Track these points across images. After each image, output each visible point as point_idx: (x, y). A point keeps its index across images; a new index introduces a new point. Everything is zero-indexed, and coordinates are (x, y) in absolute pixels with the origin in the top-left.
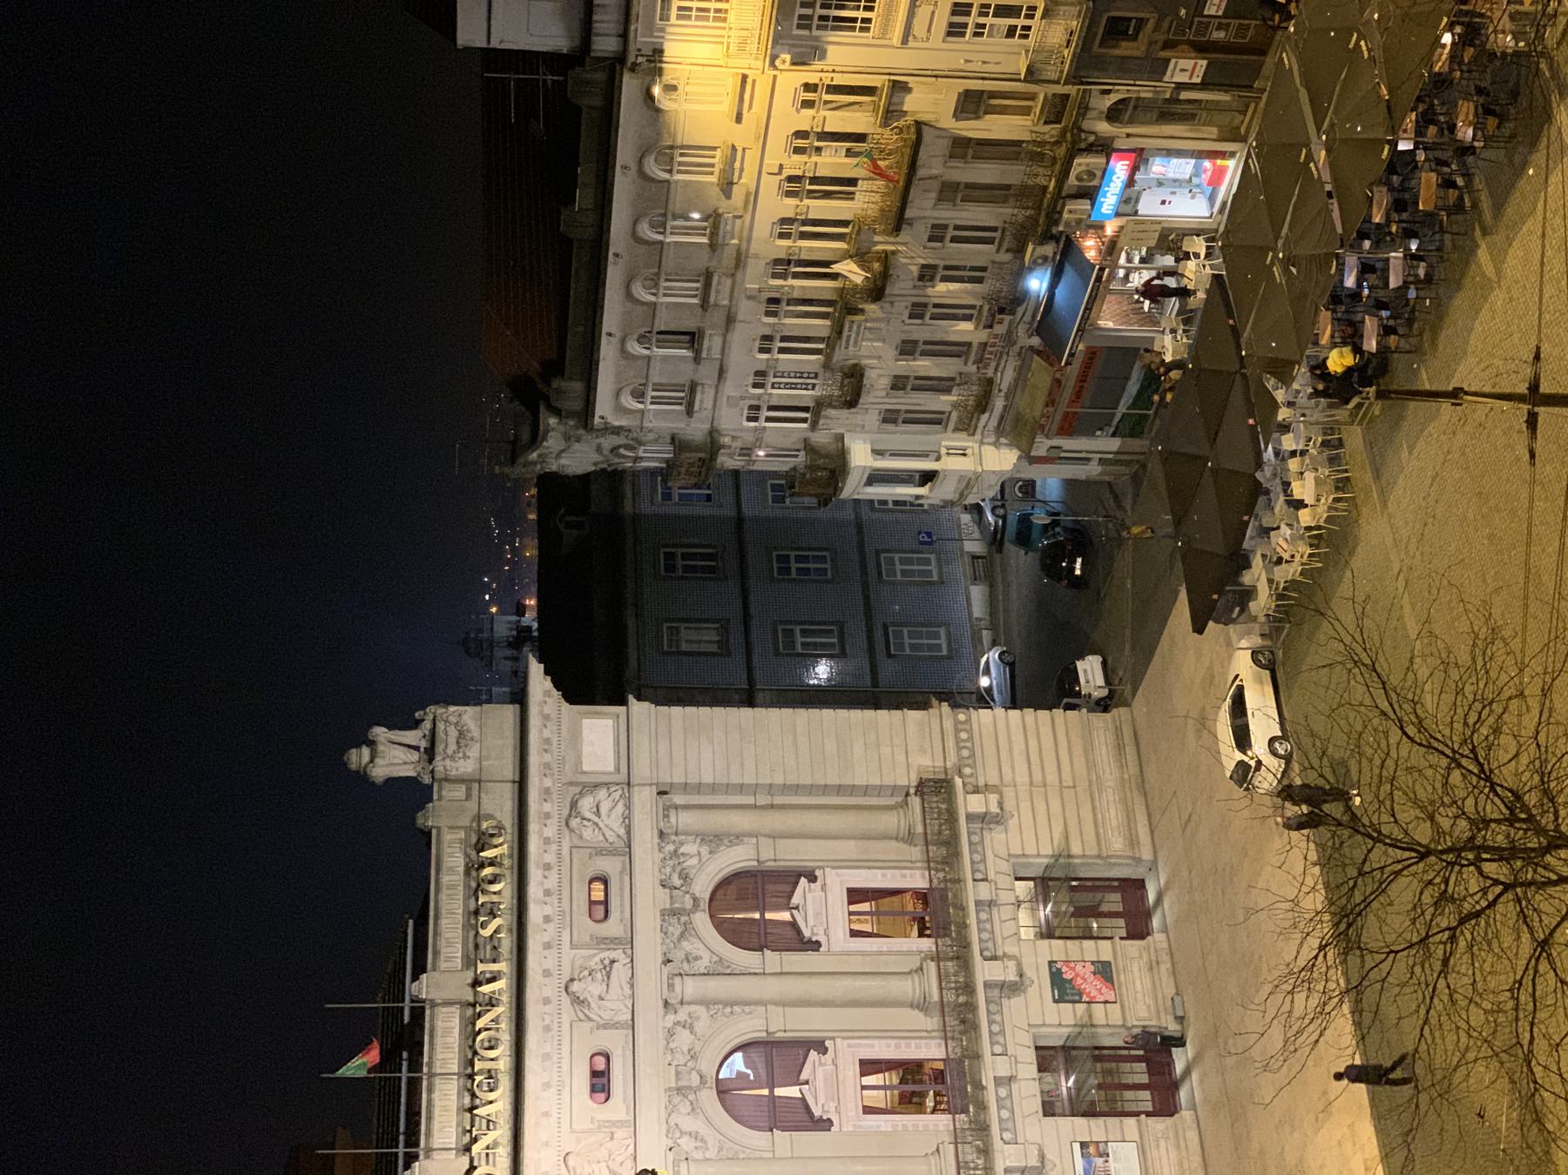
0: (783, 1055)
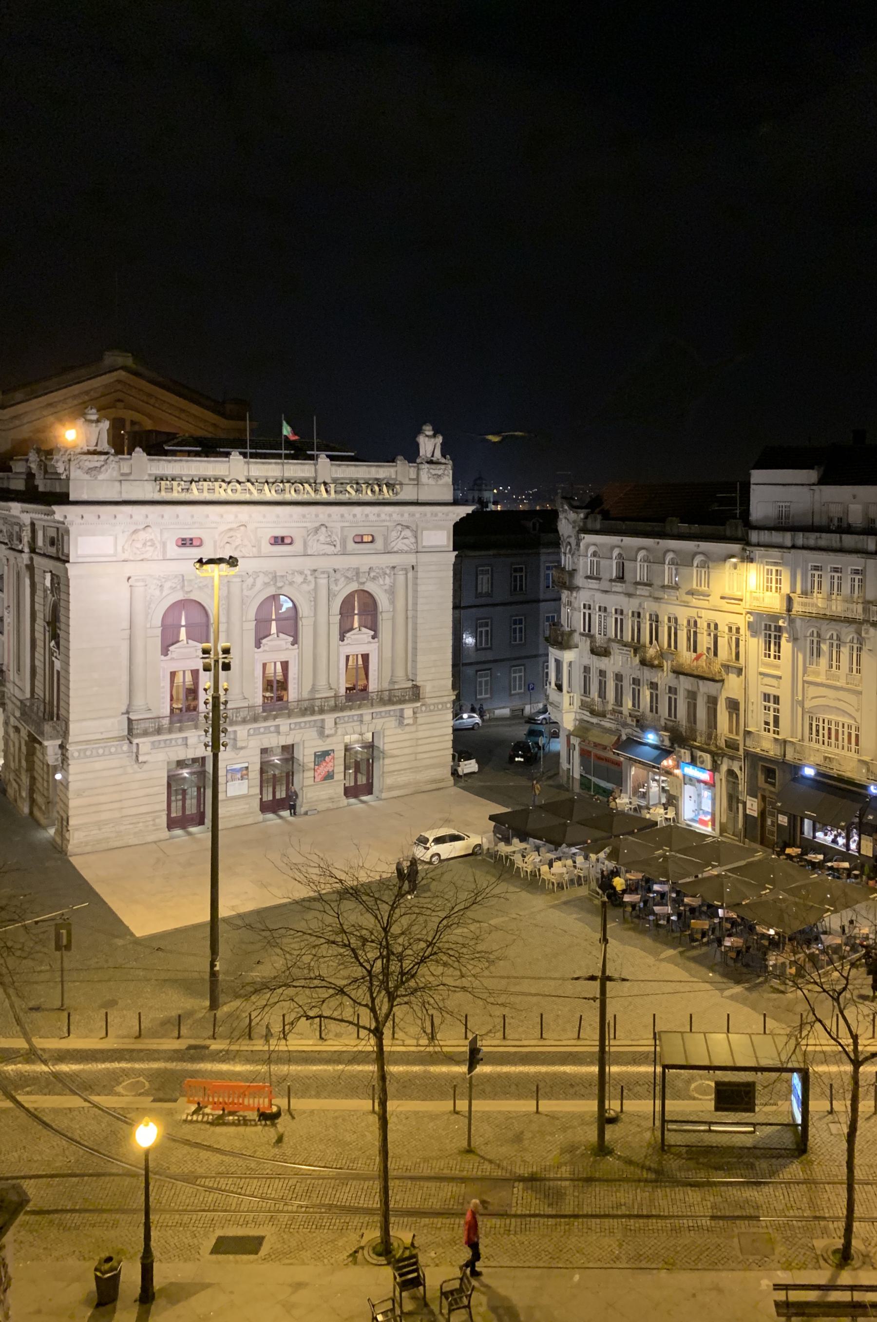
0: (291, 625)
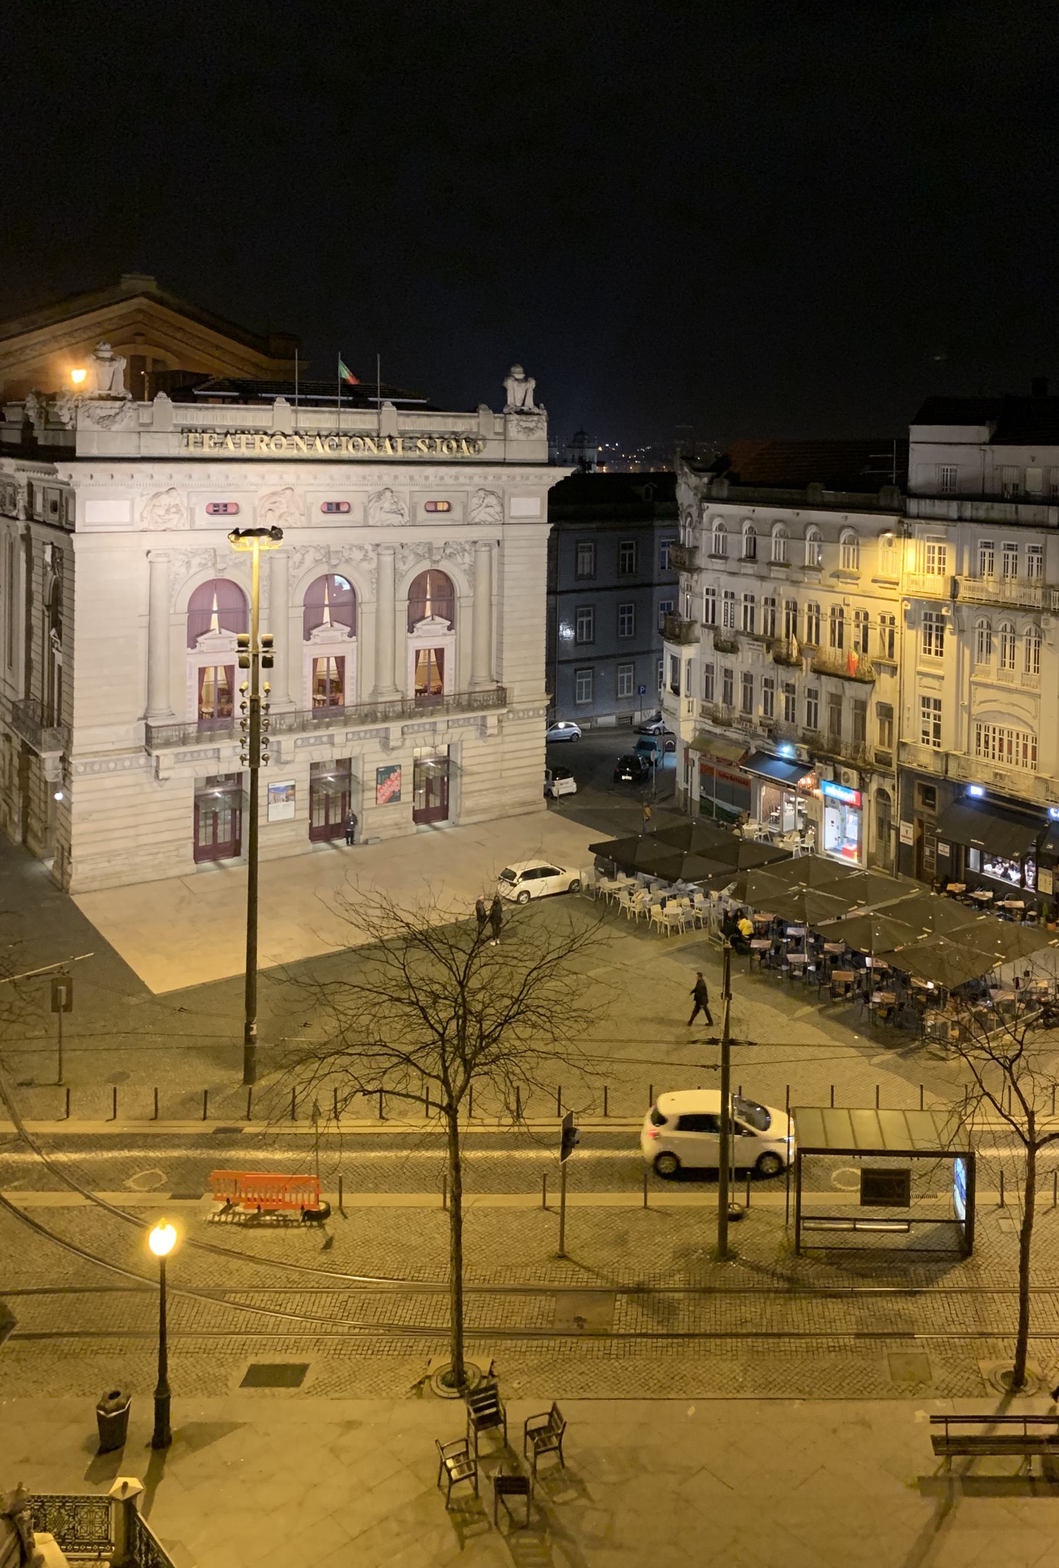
0: (348, 611)
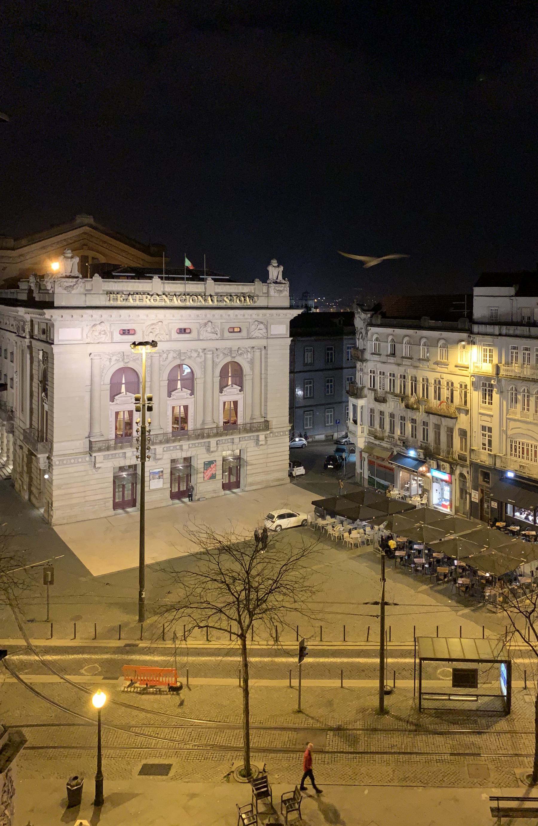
0: (190, 383)
